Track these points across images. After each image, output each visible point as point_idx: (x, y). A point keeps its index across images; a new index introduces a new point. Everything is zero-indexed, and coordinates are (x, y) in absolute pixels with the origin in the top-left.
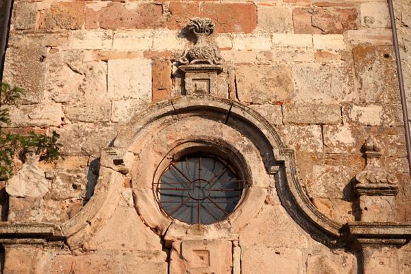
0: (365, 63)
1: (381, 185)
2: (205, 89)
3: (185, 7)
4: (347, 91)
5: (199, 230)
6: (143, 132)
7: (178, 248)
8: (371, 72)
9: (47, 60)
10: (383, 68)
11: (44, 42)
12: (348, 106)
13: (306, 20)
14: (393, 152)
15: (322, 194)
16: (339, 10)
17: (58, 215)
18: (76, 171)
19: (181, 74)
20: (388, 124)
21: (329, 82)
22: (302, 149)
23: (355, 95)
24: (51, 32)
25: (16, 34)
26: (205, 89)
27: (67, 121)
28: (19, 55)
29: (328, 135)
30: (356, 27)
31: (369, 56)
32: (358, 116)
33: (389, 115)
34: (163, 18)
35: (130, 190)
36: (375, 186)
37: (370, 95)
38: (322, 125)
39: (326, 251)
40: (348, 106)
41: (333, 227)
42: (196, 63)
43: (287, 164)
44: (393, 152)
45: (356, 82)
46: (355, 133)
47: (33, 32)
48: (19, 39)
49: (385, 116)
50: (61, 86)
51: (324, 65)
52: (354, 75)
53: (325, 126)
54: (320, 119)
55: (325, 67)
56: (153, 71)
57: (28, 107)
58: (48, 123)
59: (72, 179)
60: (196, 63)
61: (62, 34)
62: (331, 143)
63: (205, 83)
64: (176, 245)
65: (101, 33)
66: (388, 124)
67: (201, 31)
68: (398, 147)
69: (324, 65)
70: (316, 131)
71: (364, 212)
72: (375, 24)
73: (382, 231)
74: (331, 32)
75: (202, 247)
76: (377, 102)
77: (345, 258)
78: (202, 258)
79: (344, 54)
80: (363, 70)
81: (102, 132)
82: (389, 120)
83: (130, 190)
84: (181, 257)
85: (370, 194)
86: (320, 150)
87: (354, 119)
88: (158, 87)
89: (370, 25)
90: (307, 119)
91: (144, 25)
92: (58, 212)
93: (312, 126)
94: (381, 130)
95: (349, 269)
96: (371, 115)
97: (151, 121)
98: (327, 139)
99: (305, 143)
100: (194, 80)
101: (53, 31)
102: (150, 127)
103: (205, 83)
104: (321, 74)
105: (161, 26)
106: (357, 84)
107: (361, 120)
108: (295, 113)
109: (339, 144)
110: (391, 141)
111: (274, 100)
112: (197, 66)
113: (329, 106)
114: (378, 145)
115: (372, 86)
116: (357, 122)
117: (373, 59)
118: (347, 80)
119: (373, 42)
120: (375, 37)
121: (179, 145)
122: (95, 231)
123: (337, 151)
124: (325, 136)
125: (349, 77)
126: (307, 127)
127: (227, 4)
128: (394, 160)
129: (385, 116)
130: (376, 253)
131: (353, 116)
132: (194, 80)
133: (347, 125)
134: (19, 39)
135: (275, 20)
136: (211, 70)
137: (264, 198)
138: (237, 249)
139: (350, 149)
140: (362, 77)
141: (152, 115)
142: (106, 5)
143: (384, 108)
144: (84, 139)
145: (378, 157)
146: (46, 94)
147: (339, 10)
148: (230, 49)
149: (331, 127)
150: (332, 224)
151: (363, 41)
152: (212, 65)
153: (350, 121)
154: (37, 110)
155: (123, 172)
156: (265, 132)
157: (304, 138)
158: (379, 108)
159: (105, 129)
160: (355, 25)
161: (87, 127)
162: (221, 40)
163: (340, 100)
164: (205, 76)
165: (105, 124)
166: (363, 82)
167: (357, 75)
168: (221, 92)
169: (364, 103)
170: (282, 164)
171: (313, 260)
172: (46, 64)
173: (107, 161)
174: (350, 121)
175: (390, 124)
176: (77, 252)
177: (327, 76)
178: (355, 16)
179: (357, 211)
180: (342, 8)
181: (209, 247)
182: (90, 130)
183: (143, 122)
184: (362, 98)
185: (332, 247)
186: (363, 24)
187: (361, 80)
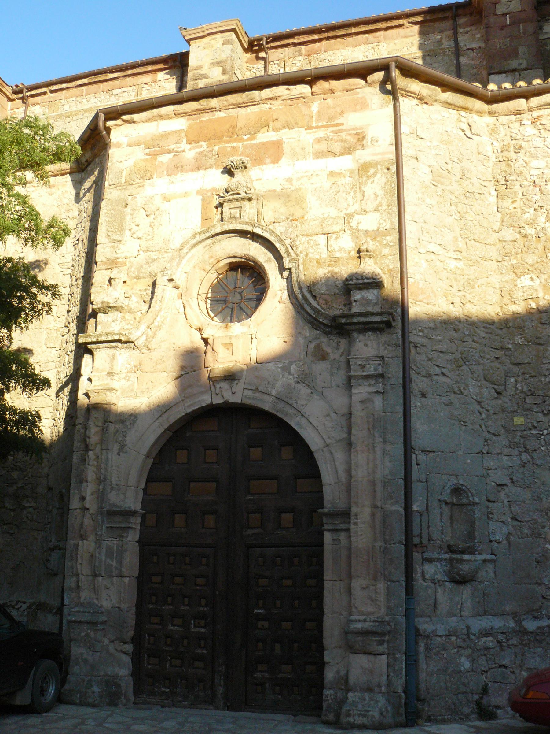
0: (369, 177)
1: (366, 281)
2: (238, 215)
3: (229, 149)
4: (351, 204)
5: (226, 328)
6: (190, 255)
7: (211, 344)
9: (128, 206)
11: (127, 193)
12: (350, 216)
13: (323, 147)
14: (386, 251)
15: (323, 292)
16: (350, 134)
17: (131, 325)
18: (145, 290)
19: (221, 205)
20: (383, 228)
21: (336, 197)
22: (310, 255)
23: (356, 207)
24: (132, 184)
25: (109, 189)
26: (238, 215)
27: (141, 252)
28: (111, 204)
29: (332, 242)
31: (372, 171)
32: (358, 223)
33: (385, 220)
34: (212, 161)
35: (180, 301)
36: (361, 282)
37: (370, 206)
39: (324, 340)
40: (350, 216)
41: (326, 318)
42: (231, 195)
43: (293, 270)
44: (386, 251)
45: (359, 195)
47: (120, 186)
48: (111, 193)
49: (382, 221)
50: (138, 226)
51: (334, 184)
52: (358, 190)
53: (329, 235)
54: (326, 230)
55: (335, 185)
56: (203, 205)
57: (116, 244)
58: (128, 255)
59: (143, 296)
60: (231, 195)
61: (140, 185)
62: (334, 249)
63: (238, 211)
64: (210, 341)
65: (167, 178)
66: (383, 228)
67: (236, 168)
68: (391, 246)
69: (334, 184)
70: (322, 239)
71: (354, 304)
73: (362, 319)
74: (342, 154)
75: (228, 341)
76: (376, 210)
77: (338, 343)
78: (229, 349)
79: (351, 172)
80: (366, 183)
81: (164, 258)
82: (384, 224)
83: (180, 301)
84: (213, 350)
85: (360, 289)
87: (355, 227)
88: (206, 219)
89: (375, 144)
91: (198, 168)
92: (132, 322)
93: (319, 236)
94: (377, 234)
95: (342, 351)
97: (194, 246)
98: (331, 246)
99: (313, 251)
100: (230, 209)
101: (134, 183)
102: (194, 251)
103: (238, 211)
104: (331, 191)
105: (210, 167)
107: (361, 227)
108: (307, 226)
109: (340, 250)
110: (385, 242)
111: (291, 218)
112: (231, 197)
113: (334, 218)
115: (373, 196)
117: (375, 174)
118: (352, 193)
119: (377, 158)
120: (379, 154)
121: (218, 262)
122: (155, 334)
123: (338, 255)
124: (329, 243)
125: (354, 191)
126: (315, 238)
127: (260, 143)
128: (386, 258)
129: (382, 221)
130: (361, 337)
131: (354, 224)
132: (230, 209)
133: (348, 232)
134: (111, 193)
136: (243, 199)
137: (278, 299)
138: (254, 341)
139: (350, 252)
140: (364, 190)
141: (194, 241)
142: (172, 157)
143: (382, 214)
144: (152, 264)
145: (370, 256)
146: (128, 233)
147: (350, 134)
148: (260, 179)
149: (334, 236)
150: (326, 316)
151: (368, 159)
152: (243, 195)
153: (351, 228)
154: (121, 246)
155: (176, 287)
157: (312, 247)
158: (377, 215)
159: (166, 255)
160: (363, 146)
161: (154, 255)
162: (254, 172)
163: (345, 212)
164: (238, 204)
165: (166, 251)
166: (365, 194)
167: (360, 188)
168: (250, 217)
170: (290, 269)
171: (312, 346)
172: (128, 210)
173: (162, 281)
174: (351, 228)
175: (385, 228)
176: (144, 350)
177: (335, 193)
178: (364, 138)
179: (349, 304)
181: (233, 341)
182: (155, 257)
183: (188, 246)
184: (363, 208)
185: (327, 334)
186: (369, 143)
187: (364, 192)
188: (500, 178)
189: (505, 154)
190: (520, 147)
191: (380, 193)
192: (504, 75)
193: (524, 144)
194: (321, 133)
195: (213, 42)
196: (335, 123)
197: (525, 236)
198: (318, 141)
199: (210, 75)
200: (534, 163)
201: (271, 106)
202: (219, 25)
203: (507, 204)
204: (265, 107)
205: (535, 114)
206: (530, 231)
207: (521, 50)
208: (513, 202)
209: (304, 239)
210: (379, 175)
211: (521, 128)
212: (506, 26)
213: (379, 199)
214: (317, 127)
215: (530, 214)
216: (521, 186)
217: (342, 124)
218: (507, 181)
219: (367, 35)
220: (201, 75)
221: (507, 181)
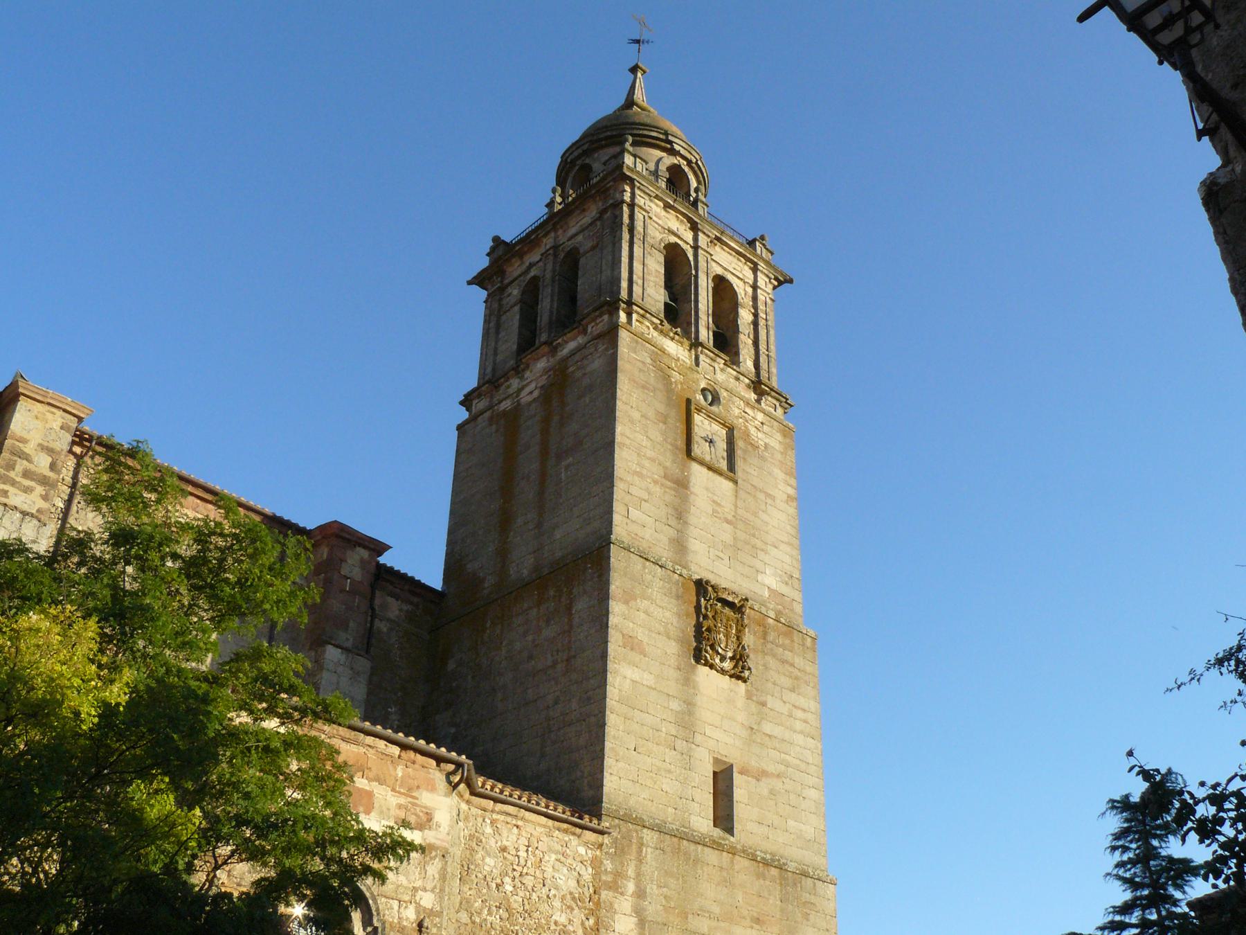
0: (431, 858)
8: (433, 868)
10: (440, 866)
23: (418, 884)
29: (402, 910)
30: (430, 828)
31: (434, 854)
37: (429, 887)
38: (400, 902)
40: (415, 889)
43: (380, 930)
45: (423, 872)
46: (417, 912)
70: (395, 904)
72: (441, 829)
76: (432, 891)
86: (396, 921)
90: (393, 895)
96: (427, 900)
106: (423, 875)
107: (422, 903)
109: (407, 919)
113: (406, 888)
114: (429, 926)
116: (419, 904)
119: (438, 843)
120: (439, 839)
123: (405, 923)
131: (418, 898)
133: (413, 904)
135: (384, 809)
140: (428, 869)
149: (404, 905)
153: (416, 903)
156: (371, 902)
169: (425, 890)
174: (416, 903)
180: (423, 810)
188: (464, 863)
189: (470, 843)
190: (481, 841)
191: (437, 876)
192: (340, 650)
193: (484, 840)
194: (402, 800)
195: (49, 416)
196: (413, 794)
197: (474, 923)
198: (400, 806)
199: (35, 459)
200: (488, 860)
201: (367, 752)
202: (68, 402)
203: (465, 889)
204: (362, 750)
205: (495, 816)
206: (478, 920)
207: (352, 624)
208: (470, 889)
209: (383, 899)
210: (437, 859)
211: (484, 824)
212: (345, 590)
213: (435, 881)
214: (399, 792)
215: (478, 904)
216: (476, 876)
217: (417, 799)
218: (468, 868)
219: (199, 501)
220: (24, 453)
221: (468, 868)
